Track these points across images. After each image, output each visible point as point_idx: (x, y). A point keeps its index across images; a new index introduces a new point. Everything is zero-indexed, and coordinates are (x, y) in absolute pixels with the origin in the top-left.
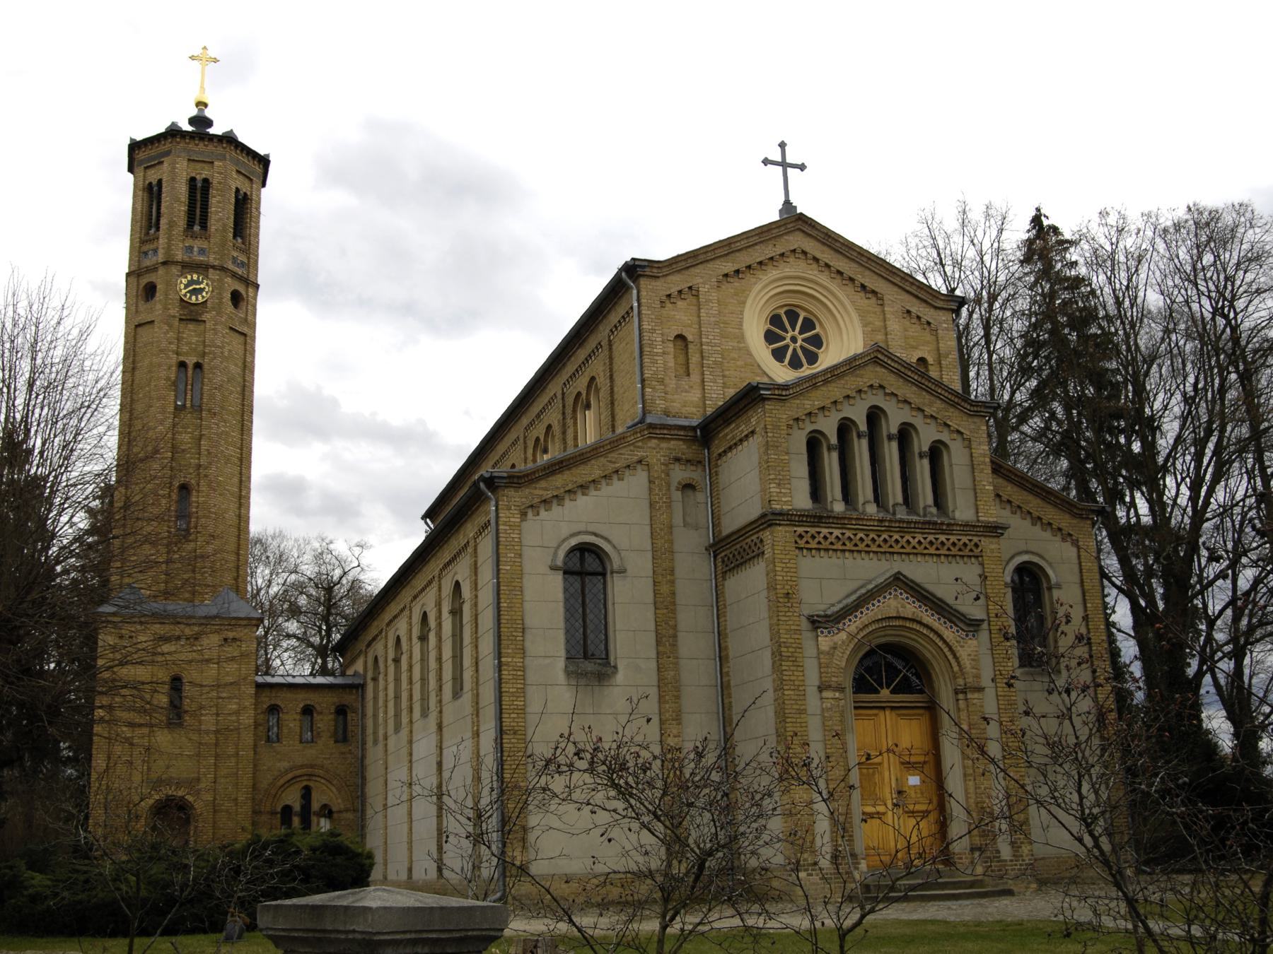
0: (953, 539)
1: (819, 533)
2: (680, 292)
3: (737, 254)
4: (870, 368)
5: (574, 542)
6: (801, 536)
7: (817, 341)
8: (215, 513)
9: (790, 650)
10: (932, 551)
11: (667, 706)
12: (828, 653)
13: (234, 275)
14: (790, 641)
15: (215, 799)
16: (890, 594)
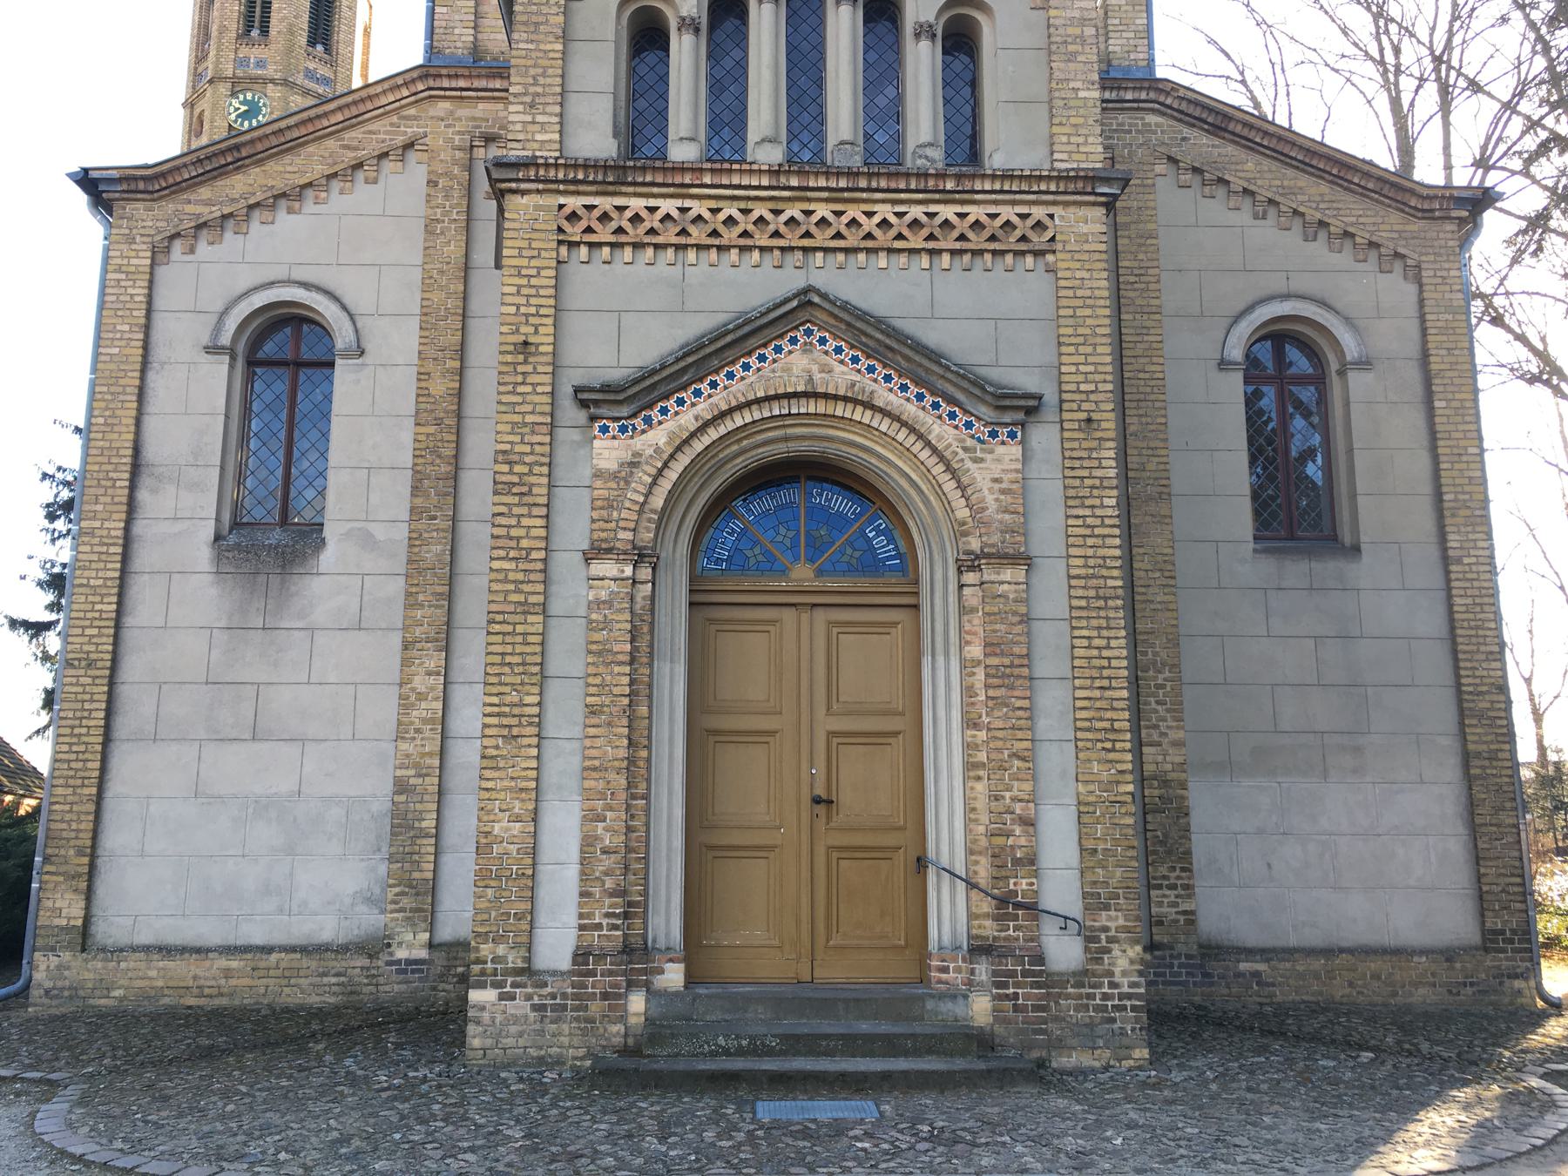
0: (976, 212)
1: (621, 209)
5: (259, 300)
6: (573, 217)
9: (518, 469)
10: (916, 241)
12: (614, 476)
14: (518, 448)
16: (794, 341)
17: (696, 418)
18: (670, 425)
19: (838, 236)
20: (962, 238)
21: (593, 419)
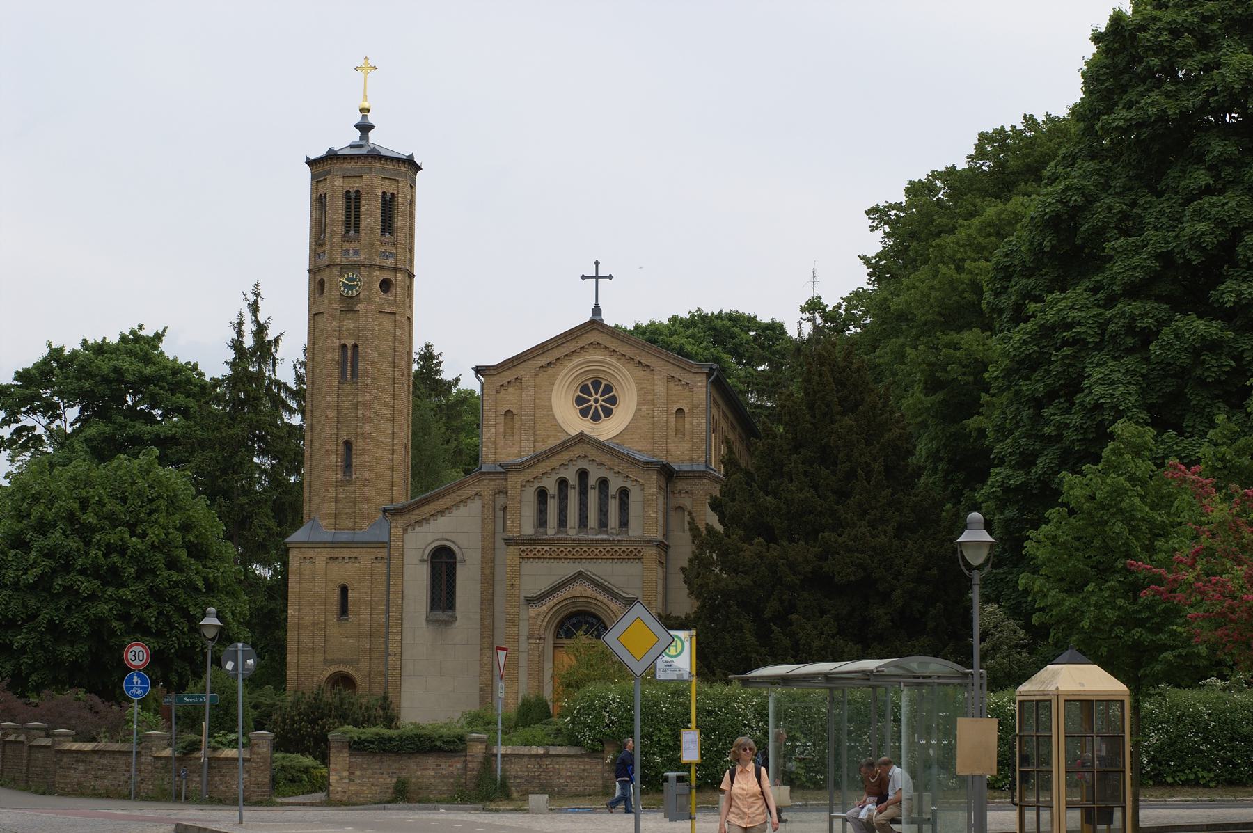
0: (623, 548)
2: (509, 382)
4: (580, 445)
5: (434, 545)
6: (523, 551)
7: (613, 400)
8: (369, 462)
10: (608, 556)
13: (382, 268)
15: (370, 674)
19: (589, 555)
20: (620, 555)
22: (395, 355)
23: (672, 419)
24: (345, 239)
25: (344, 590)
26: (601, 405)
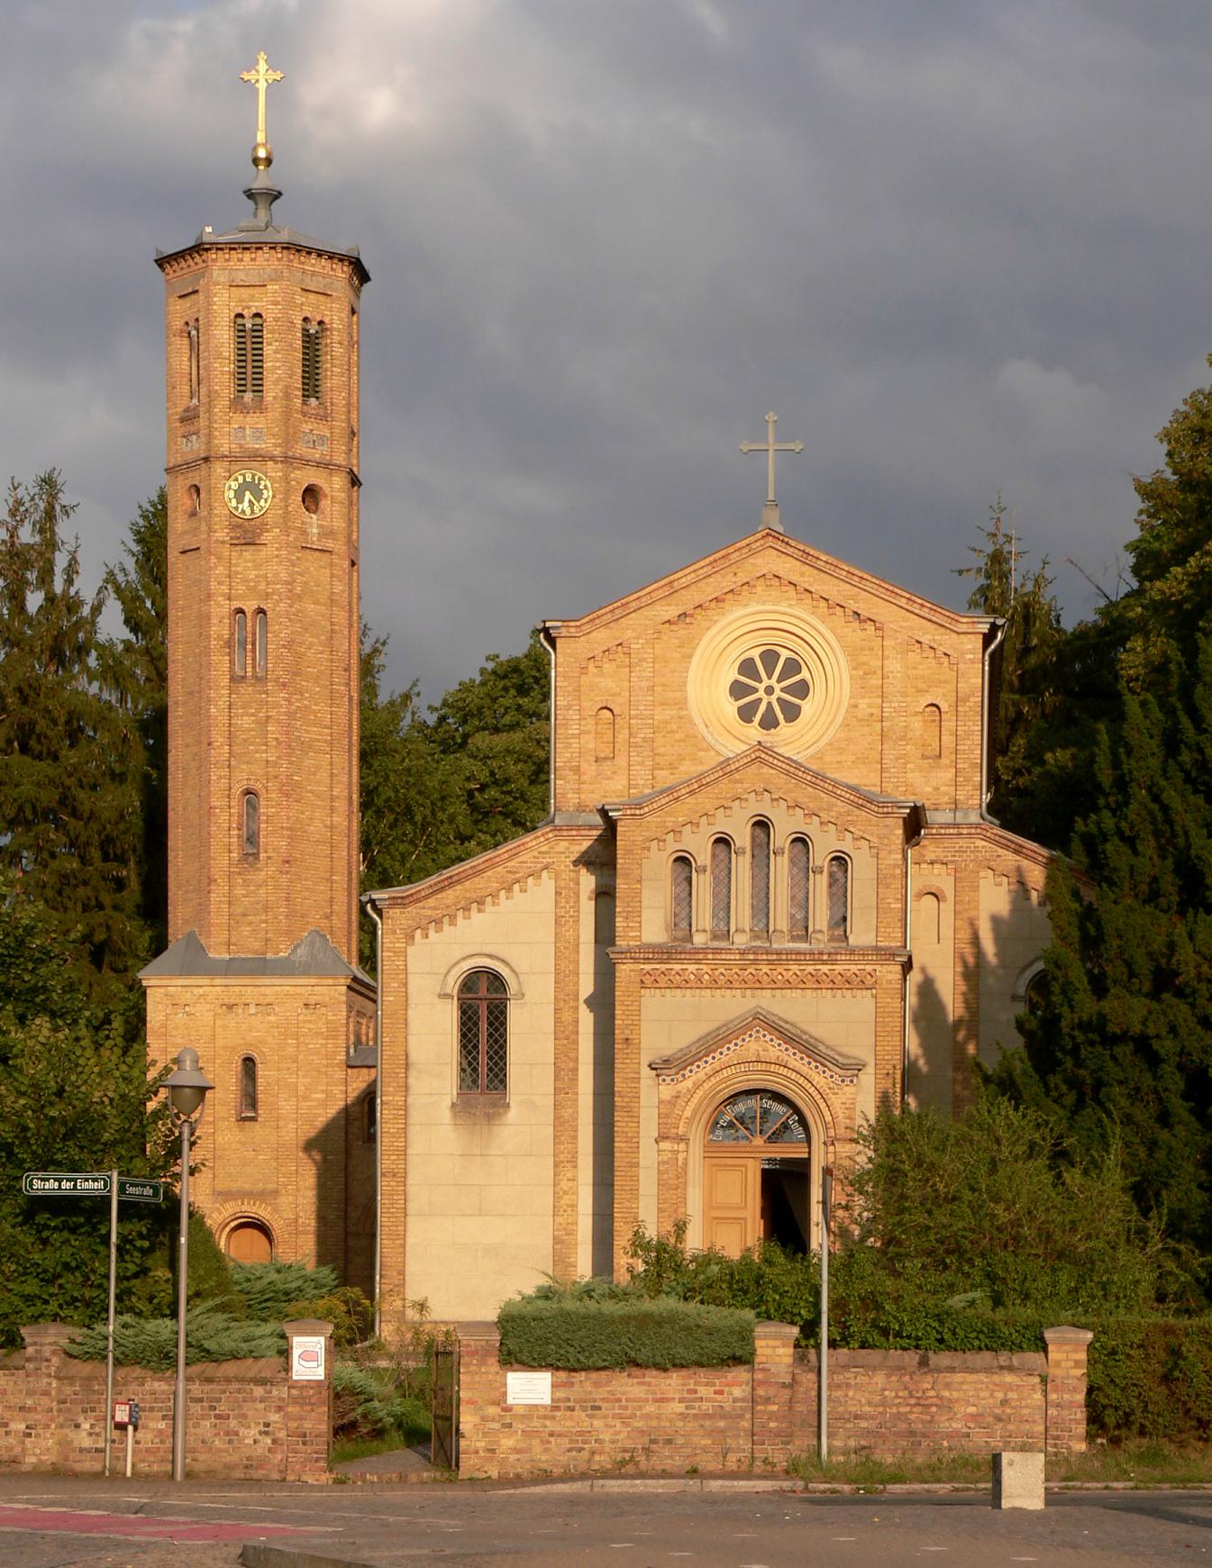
3: (683, 592)
9: (626, 1100)
11: (562, 1147)
12: (669, 1102)
13: (306, 462)
14: (625, 1090)
17: (706, 1074)
18: (694, 1078)
21: (658, 1075)
22: (333, 631)
23: (917, 723)
24: (237, 405)
25: (249, 1063)
26: (779, 700)
